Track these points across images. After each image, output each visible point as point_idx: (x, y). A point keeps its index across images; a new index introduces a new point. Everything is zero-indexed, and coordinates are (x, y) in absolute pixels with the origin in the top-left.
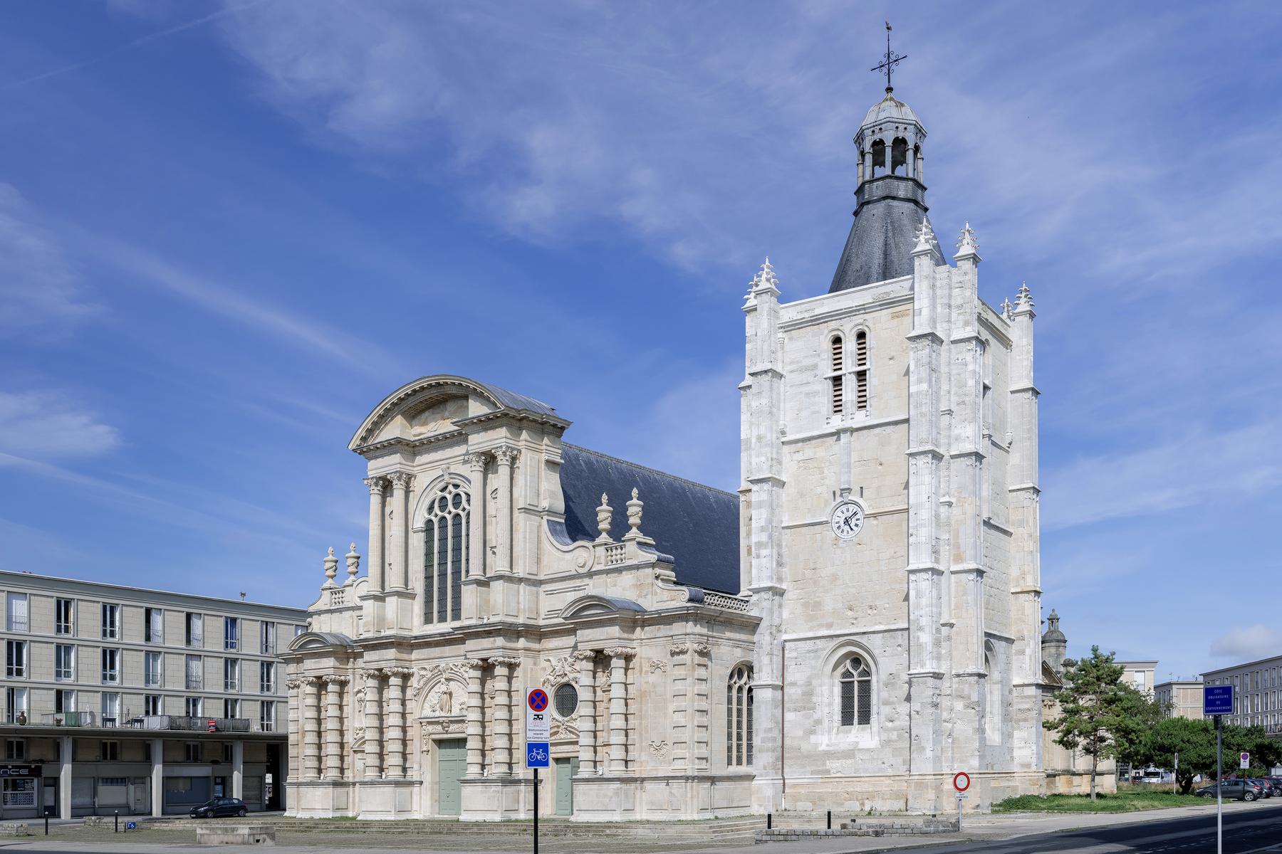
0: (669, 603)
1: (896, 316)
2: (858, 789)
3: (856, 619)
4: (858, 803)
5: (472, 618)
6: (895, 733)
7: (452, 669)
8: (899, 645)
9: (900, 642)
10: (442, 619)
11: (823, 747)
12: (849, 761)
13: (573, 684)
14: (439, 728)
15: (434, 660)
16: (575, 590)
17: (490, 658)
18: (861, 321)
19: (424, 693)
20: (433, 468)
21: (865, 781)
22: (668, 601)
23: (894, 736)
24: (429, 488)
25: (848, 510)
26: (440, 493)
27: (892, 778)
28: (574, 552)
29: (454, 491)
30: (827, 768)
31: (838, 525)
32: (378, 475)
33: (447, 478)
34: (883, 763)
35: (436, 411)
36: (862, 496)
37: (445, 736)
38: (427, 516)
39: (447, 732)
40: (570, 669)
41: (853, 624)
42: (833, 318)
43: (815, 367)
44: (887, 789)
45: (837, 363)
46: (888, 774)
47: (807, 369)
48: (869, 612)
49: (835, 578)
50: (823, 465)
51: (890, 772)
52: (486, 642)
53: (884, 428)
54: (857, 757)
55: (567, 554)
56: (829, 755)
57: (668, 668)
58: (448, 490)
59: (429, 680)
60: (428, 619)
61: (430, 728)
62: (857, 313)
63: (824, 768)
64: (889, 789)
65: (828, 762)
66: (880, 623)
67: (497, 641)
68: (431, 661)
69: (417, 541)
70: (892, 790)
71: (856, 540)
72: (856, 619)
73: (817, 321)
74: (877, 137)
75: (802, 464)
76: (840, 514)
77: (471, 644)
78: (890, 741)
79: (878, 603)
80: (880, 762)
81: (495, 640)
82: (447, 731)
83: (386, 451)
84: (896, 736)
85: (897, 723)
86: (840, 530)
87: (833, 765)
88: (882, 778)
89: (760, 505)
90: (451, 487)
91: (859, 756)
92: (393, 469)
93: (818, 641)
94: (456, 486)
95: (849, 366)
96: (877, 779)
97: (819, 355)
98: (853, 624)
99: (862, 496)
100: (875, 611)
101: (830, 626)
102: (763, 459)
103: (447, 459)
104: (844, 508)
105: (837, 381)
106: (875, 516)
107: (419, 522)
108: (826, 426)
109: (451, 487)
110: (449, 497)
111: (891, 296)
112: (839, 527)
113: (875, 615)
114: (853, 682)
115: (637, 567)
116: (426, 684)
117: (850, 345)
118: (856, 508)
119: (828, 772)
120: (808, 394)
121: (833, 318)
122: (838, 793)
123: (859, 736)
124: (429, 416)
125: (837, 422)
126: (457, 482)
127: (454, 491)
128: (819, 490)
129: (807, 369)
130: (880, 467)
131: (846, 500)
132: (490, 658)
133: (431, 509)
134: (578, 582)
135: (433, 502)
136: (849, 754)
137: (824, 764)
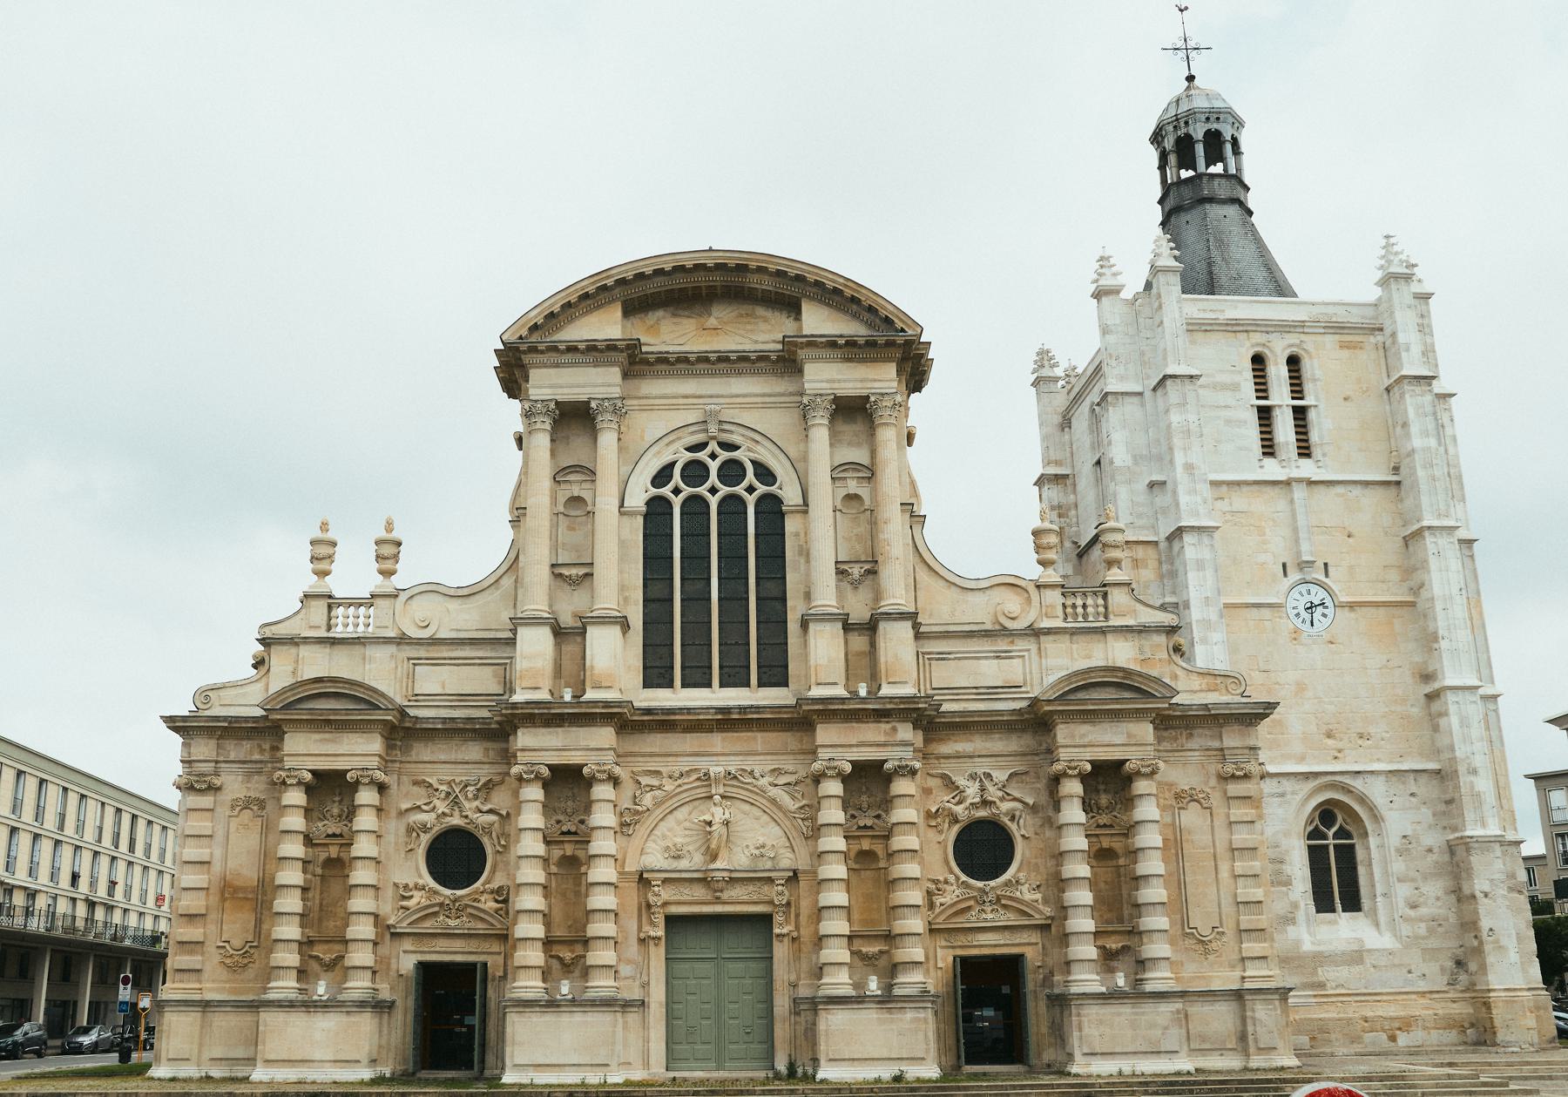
0: (1203, 695)
1: (1344, 346)
2: (1381, 1013)
3: (1340, 751)
4: (1384, 1036)
5: (835, 684)
6: (1423, 925)
7: (735, 777)
8: (1412, 795)
9: (1414, 789)
10: (697, 677)
11: (1307, 946)
12: (1356, 969)
13: (1006, 820)
14: (699, 892)
15: (679, 759)
16: (998, 657)
17: (886, 761)
18: (1298, 342)
19: (650, 821)
20: (687, 407)
21: (1389, 1001)
22: (1201, 691)
23: (1422, 929)
24: (666, 440)
25: (1309, 592)
26: (690, 456)
27: (1428, 995)
28: (988, 592)
29: (724, 455)
30: (1321, 979)
31: (1296, 611)
32: (560, 398)
33: (713, 429)
34: (1410, 972)
35: (680, 312)
36: (1327, 575)
37: (719, 909)
38: (654, 491)
39: (718, 901)
40: (1000, 794)
41: (1336, 758)
42: (1259, 329)
43: (1235, 387)
44: (1427, 1012)
45: (1262, 389)
46: (1420, 990)
47: (1224, 387)
48: (1360, 742)
49: (1301, 688)
50: (1263, 524)
51: (1423, 986)
52: (872, 732)
53: (1350, 488)
54: (1368, 961)
55: (970, 593)
56: (1320, 959)
57: (1216, 800)
58: (708, 450)
59: (669, 796)
60: (656, 675)
61: (666, 894)
62: (1292, 330)
63: (1315, 979)
64: (1431, 1012)
65: (1319, 969)
66: (1378, 760)
67: (899, 729)
68: (670, 759)
69: (635, 530)
70: (1436, 1015)
71: (1327, 637)
72: (1340, 751)
73: (1235, 327)
74: (1214, 126)
75: (1228, 517)
76: (1298, 596)
77: (826, 734)
78: (1417, 937)
79: (1372, 730)
80: (1405, 971)
81: (894, 729)
82: (718, 898)
83: (590, 358)
84: (1425, 930)
85: (1423, 911)
86: (1301, 619)
87: (1329, 974)
88: (1414, 997)
89: (1200, 565)
90: (713, 446)
91: (1368, 960)
92: (600, 392)
93: (1284, 781)
94: (733, 447)
95: (1280, 396)
96: (1405, 997)
97: (1240, 372)
98: (1336, 758)
99: (1327, 575)
100: (1369, 742)
101: (1302, 759)
102: (1199, 499)
103: (711, 397)
104: (1303, 588)
105: (1265, 414)
106: (1352, 606)
107: (638, 498)
108: (1259, 470)
109: (713, 446)
110: (714, 466)
111: (1334, 320)
112: (1298, 615)
113: (1369, 747)
114: (1327, 846)
115: (1142, 630)
116: (658, 804)
117: (1278, 372)
118: (1322, 594)
119: (1322, 985)
120: (1228, 422)
121: (1259, 329)
122: (1351, 1019)
123: (1343, 929)
124: (664, 318)
125: (1272, 469)
126: (735, 439)
127: (724, 455)
128: (1262, 558)
129: (1224, 387)
130: (1351, 540)
131: (1308, 578)
132: (886, 761)
133: (662, 477)
134: (1002, 645)
135: (672, 465)
136: (1356, 957)
137: (1314, 972)
